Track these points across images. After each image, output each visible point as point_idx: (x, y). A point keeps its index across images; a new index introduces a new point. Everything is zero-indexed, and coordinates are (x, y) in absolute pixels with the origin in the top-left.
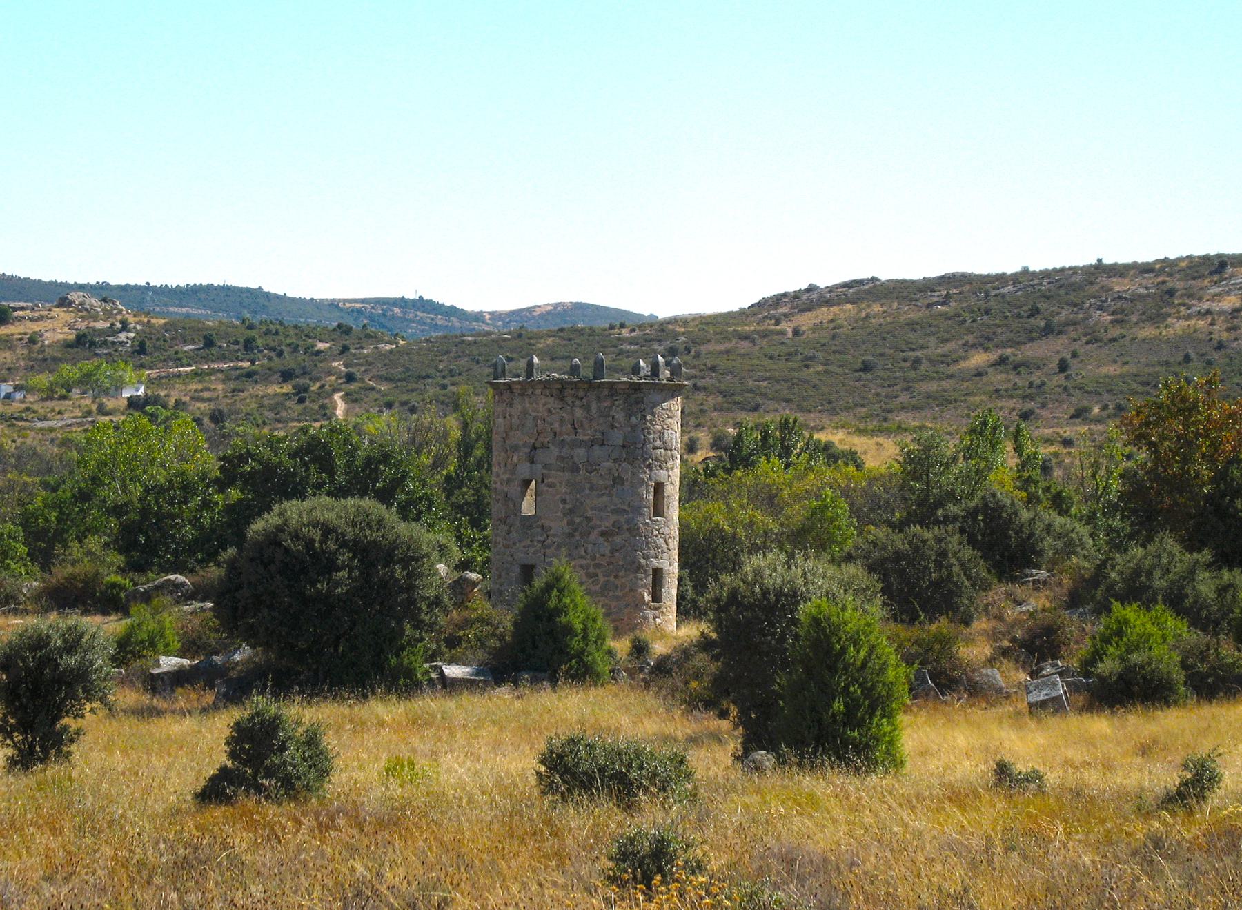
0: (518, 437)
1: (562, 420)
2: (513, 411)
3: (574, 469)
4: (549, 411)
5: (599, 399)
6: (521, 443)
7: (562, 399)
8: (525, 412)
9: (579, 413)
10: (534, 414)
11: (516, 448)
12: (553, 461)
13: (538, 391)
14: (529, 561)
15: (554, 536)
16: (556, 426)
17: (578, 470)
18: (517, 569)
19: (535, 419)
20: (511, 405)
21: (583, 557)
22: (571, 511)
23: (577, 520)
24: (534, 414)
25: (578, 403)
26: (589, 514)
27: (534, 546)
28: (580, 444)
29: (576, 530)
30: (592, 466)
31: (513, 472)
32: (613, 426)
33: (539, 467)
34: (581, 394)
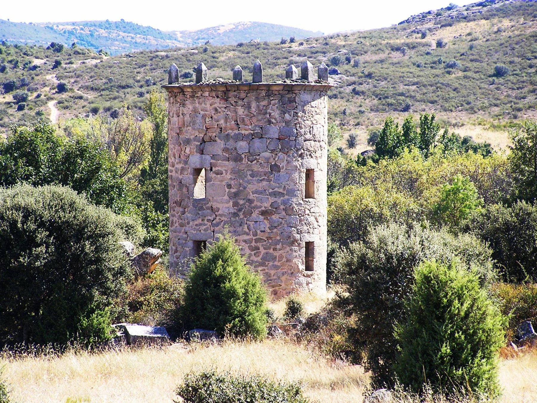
0: (190, 133)
1: (226, 119)
3: (238, 159)
4: (216, 110)
5: (257, 99)
6: (192, 137)
7: (226, 100)
8: (195, 111)
9: (241, 111)
11: (188, 142)
12: (220, 153)
13: (207, 94)
14: (198, 238)
15: (221, 215)
16: (222, 122)
17: (241, 160)
18: (191, 244)
19: (204, 117)
21: (248, 234)
22: (236, 195)
23: (241, 202)
24: (202, 113)
25: (240, 102)
26: (251, 196)
27: (205, 225)
28: (243, 137)
29: (240, 210)
30: (252, 155)
31: (186, 163)
32: (270, 122)
33: (208, 157)
34: (243, 95)
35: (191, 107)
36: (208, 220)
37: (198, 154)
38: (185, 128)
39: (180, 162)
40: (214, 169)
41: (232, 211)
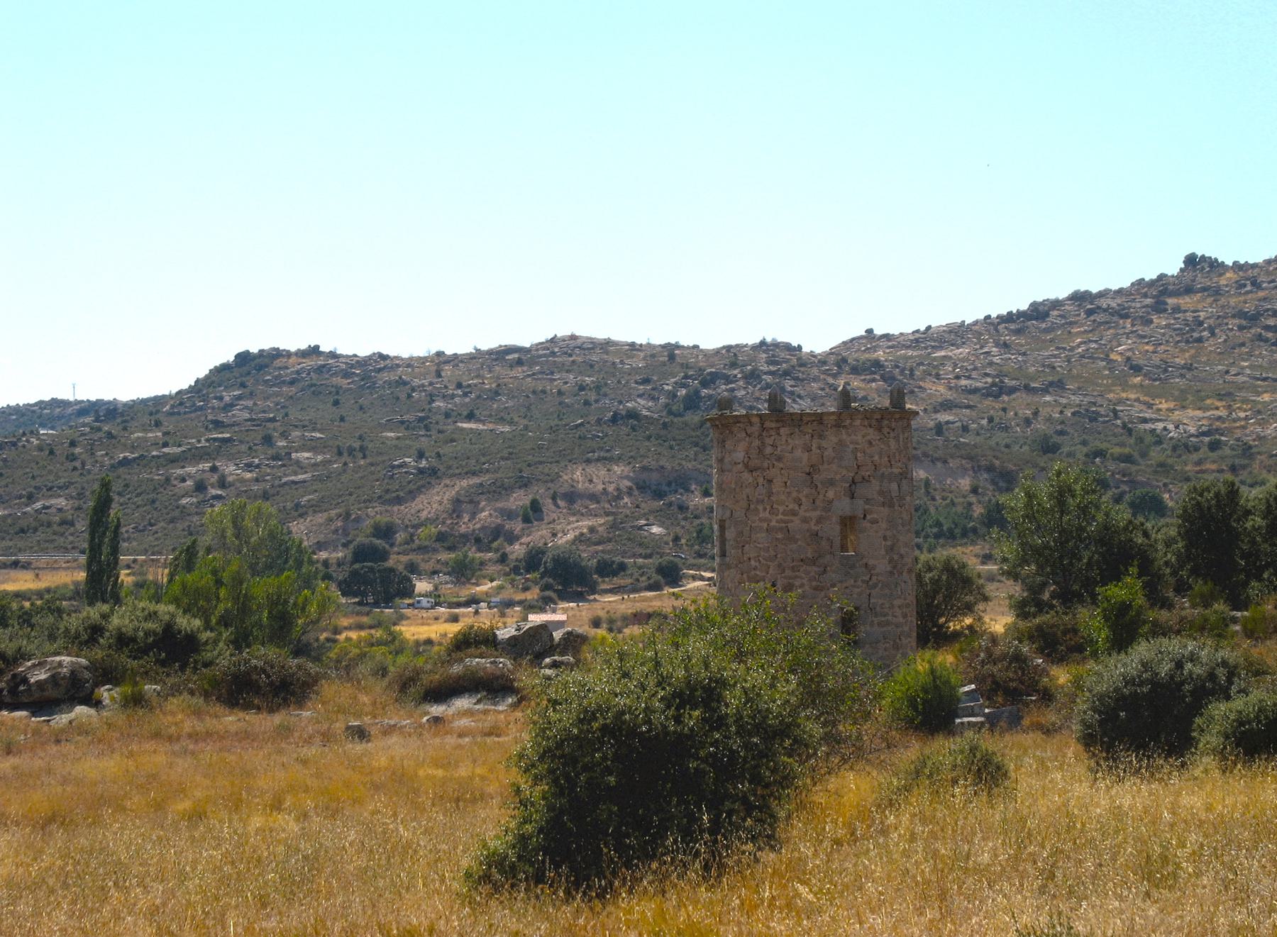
2: (824, 444)
3: (891, 505)
4: (870, 443)
6: (838, 477)
7: (880, 429)
8: (841, 443)
10: (851, 446)
11: (831, 483)
16: (876, 458)
20: (821, 437)
23: (896, 557)
24: (851, 446)
26: (902, 551)
33: (861, 502)
35: (835, 440)
36: (863, 581)
37: (847, 500)
38: (826, 466)
39: (814, 510)
40: (868, 517)
41: (889, 569)
